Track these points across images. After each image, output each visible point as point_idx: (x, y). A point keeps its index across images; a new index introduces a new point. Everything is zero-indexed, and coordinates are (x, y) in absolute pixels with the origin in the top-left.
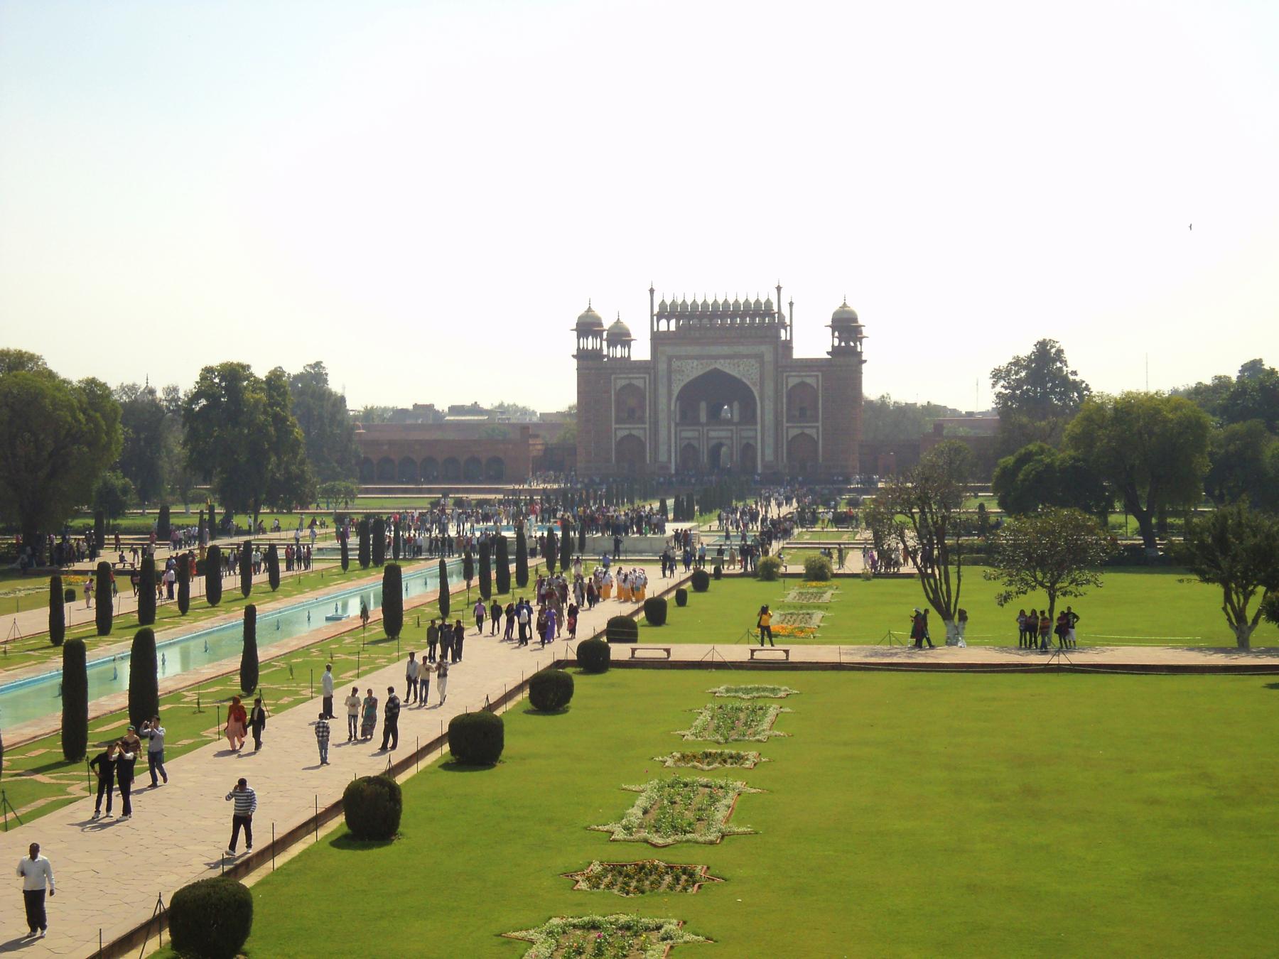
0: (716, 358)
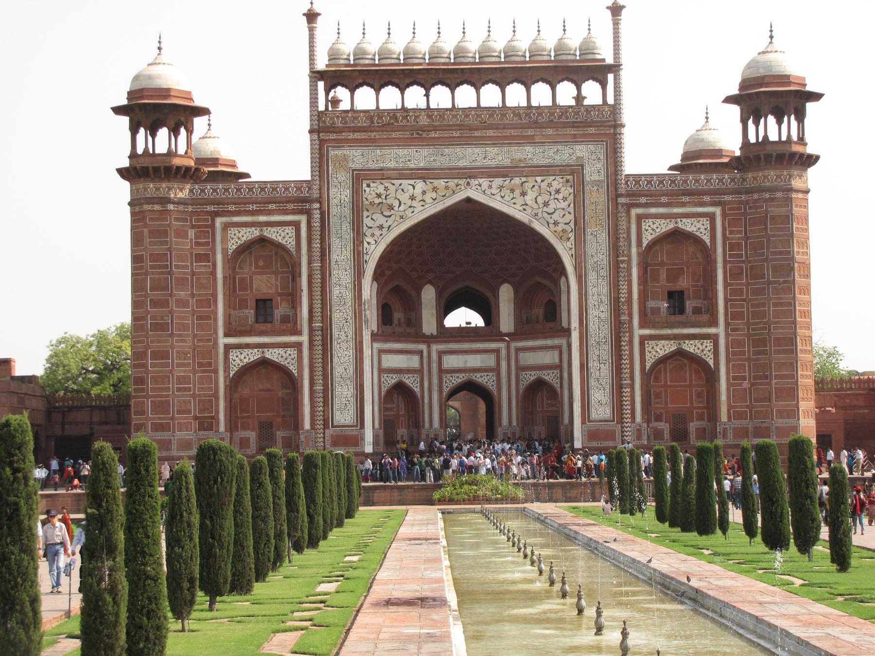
0: (469, 174)
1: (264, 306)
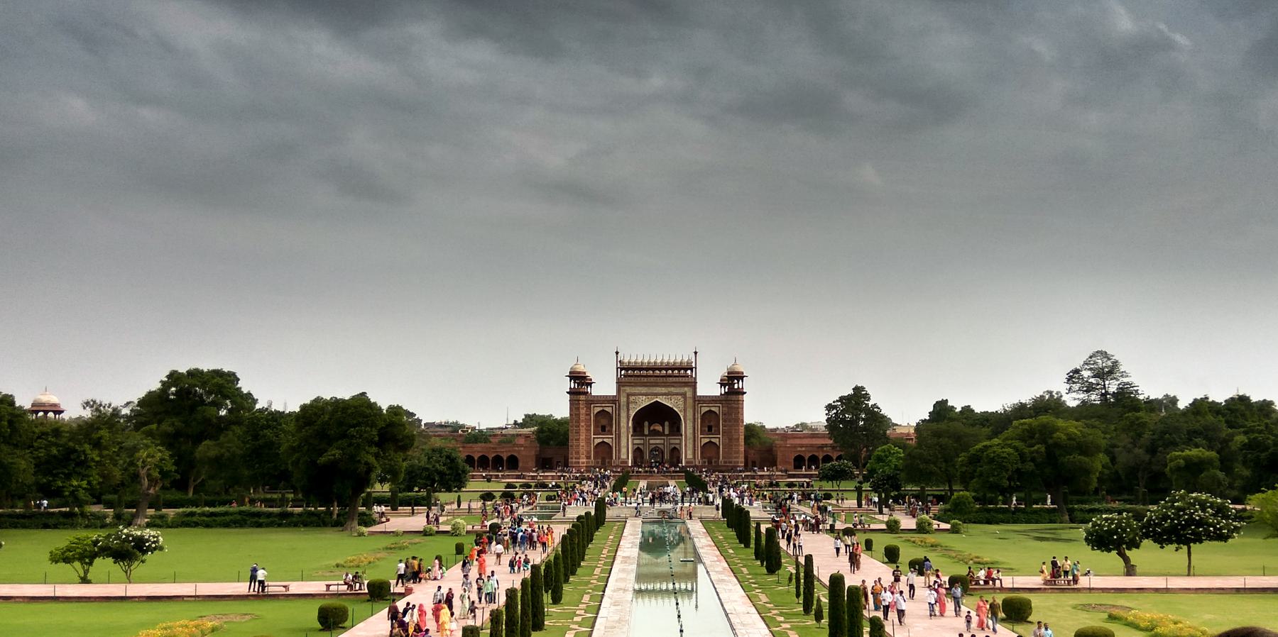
1: (603, 428)
